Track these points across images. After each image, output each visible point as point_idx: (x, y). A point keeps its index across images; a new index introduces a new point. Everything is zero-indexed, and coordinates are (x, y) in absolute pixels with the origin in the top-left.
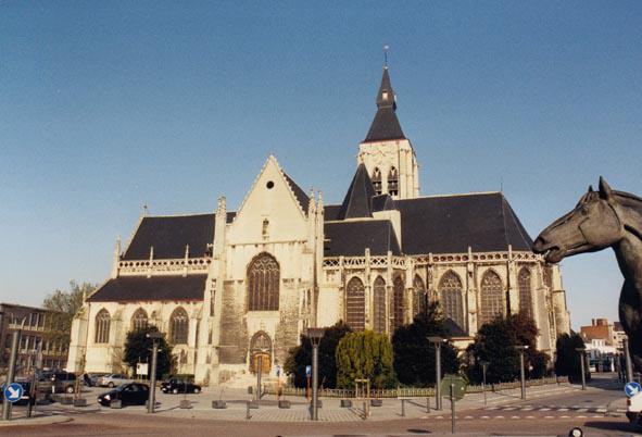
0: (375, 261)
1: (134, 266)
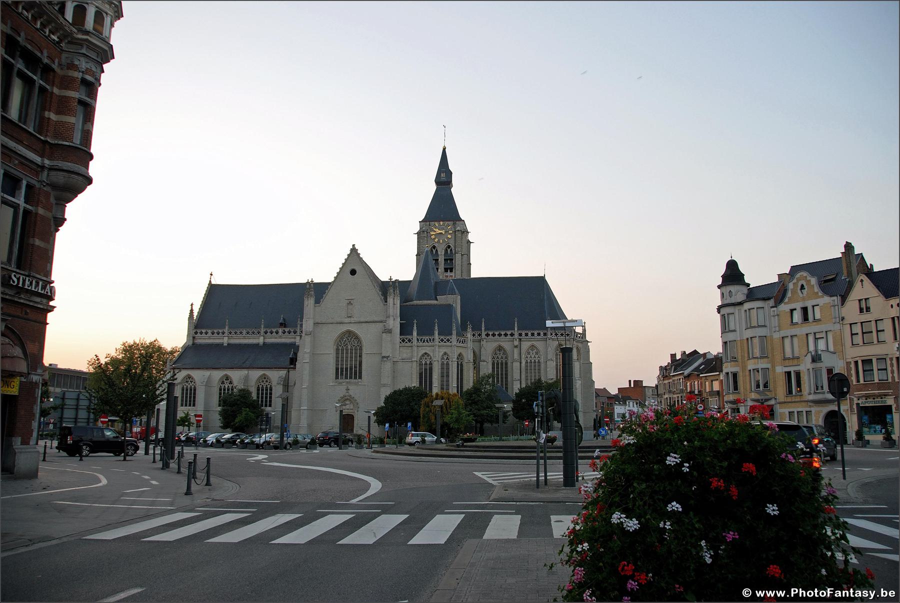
0: (442, 340)
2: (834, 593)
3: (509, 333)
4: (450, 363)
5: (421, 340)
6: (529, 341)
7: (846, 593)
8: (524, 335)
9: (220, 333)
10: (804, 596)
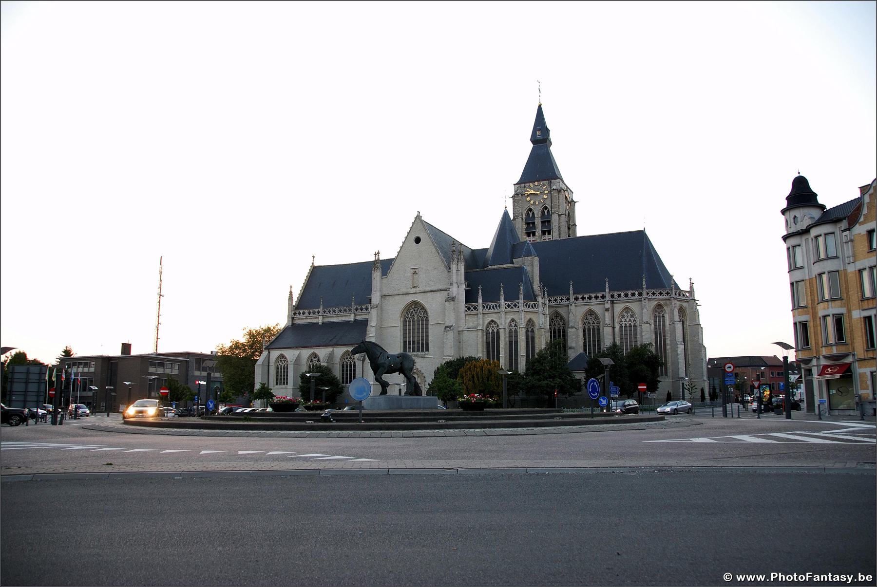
0: (509, 306)
1: (307, 314)
2: (813, 578)
3: (600, 295)
4: (518, 330)
5: (487, 307)
6: (623, 303)
7: (824, 577)
8: (616, 296)
9: (315, 312)
10: (784, 580)
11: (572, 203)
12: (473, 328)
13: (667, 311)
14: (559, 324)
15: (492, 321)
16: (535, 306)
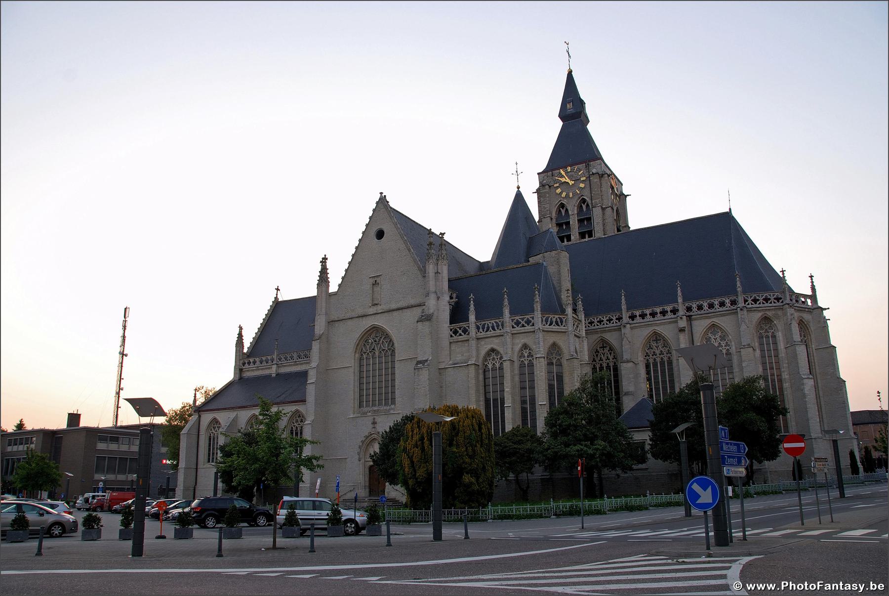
0: (518, 323)
1: (258, 363)
3: (668, 308)
11: (622, 197)
12: (462, 363)
13: (779, 328)
14: (608, 359)
15: (493, 350)
16: (562, 322)
